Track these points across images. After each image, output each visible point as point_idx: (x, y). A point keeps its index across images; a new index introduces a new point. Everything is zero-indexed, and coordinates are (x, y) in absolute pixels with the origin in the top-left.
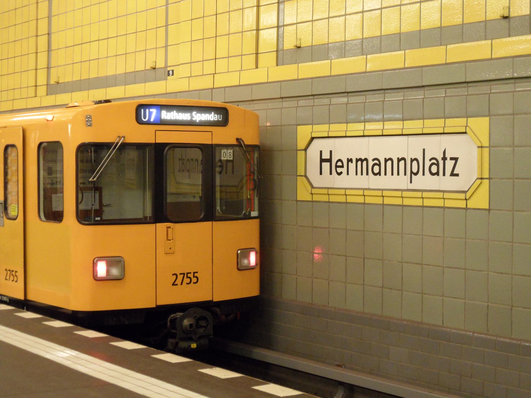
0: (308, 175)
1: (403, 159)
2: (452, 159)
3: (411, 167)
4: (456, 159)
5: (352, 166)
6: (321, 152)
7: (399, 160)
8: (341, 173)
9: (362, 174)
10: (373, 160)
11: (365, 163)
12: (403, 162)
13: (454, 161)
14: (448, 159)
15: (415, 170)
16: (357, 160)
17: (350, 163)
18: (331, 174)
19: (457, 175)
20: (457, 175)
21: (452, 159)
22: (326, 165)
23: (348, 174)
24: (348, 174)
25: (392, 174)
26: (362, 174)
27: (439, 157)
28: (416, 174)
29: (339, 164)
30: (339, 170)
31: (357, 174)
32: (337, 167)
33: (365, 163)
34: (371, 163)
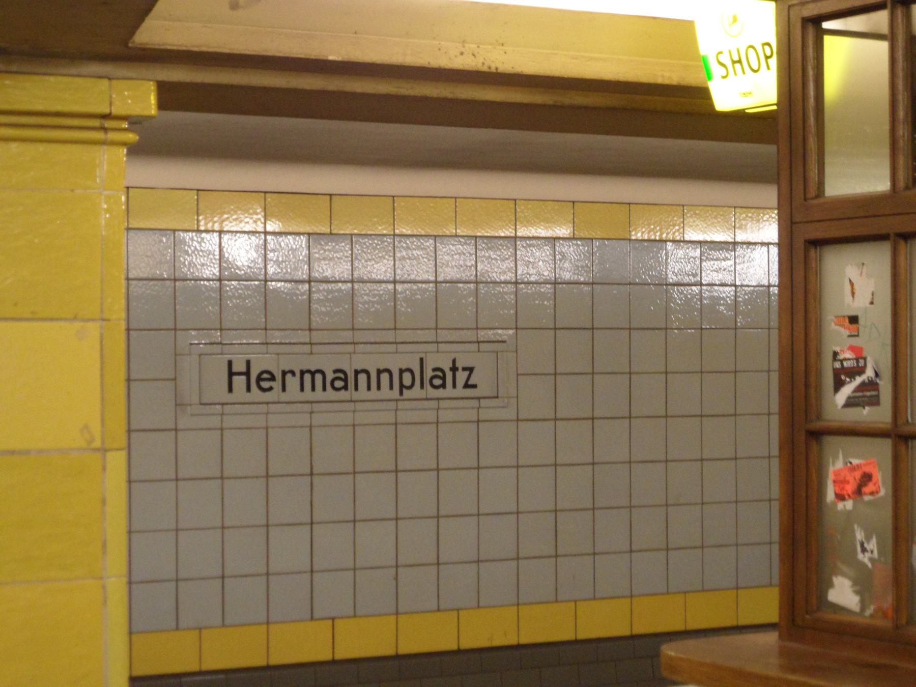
2: (464, 369)
4: (471, 370)
7: (379, 372)
11: (318, 377)
13: (467, 373)
14: (460, 369)
16: (302, 373)
21: (464, 369)
23: (284, 389)
24: (284, 389)
29: (265, 376)
30: (265, 385)
31: (302, 389)
33: (318, 377)
34: (330, 376)
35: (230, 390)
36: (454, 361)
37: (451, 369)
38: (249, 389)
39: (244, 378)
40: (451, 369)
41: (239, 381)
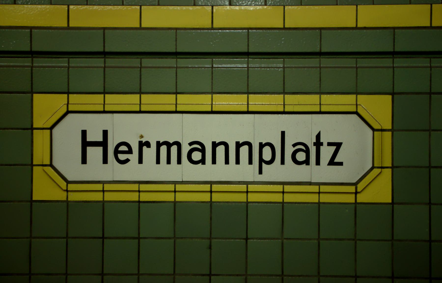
0: (54, 164)
2: (330, 144)
3: (263, 154)
4: (338, 145)
7: (238, 145)
11: (174, 149)
12: (246, 148)
13: (334, 148)
14: (325, 144)
16: (159, 145)
17: (145, 148)
20: (341, 164)
21: (330, 144)
24: (140, 161)
25: (227, 162)
26: (169, 162)
27: (310, 142)
29: (123, 148)
30: (122, 157)
31: (158, 162)
32: (117, 152)
33: (174, 149)
34: (186, 149)
35: (84, 161)
36: (318, 136)
37: (315, 144)
38: (105, 161)
39: (100, 149)
40: (315, 144)
41: (95, 153)
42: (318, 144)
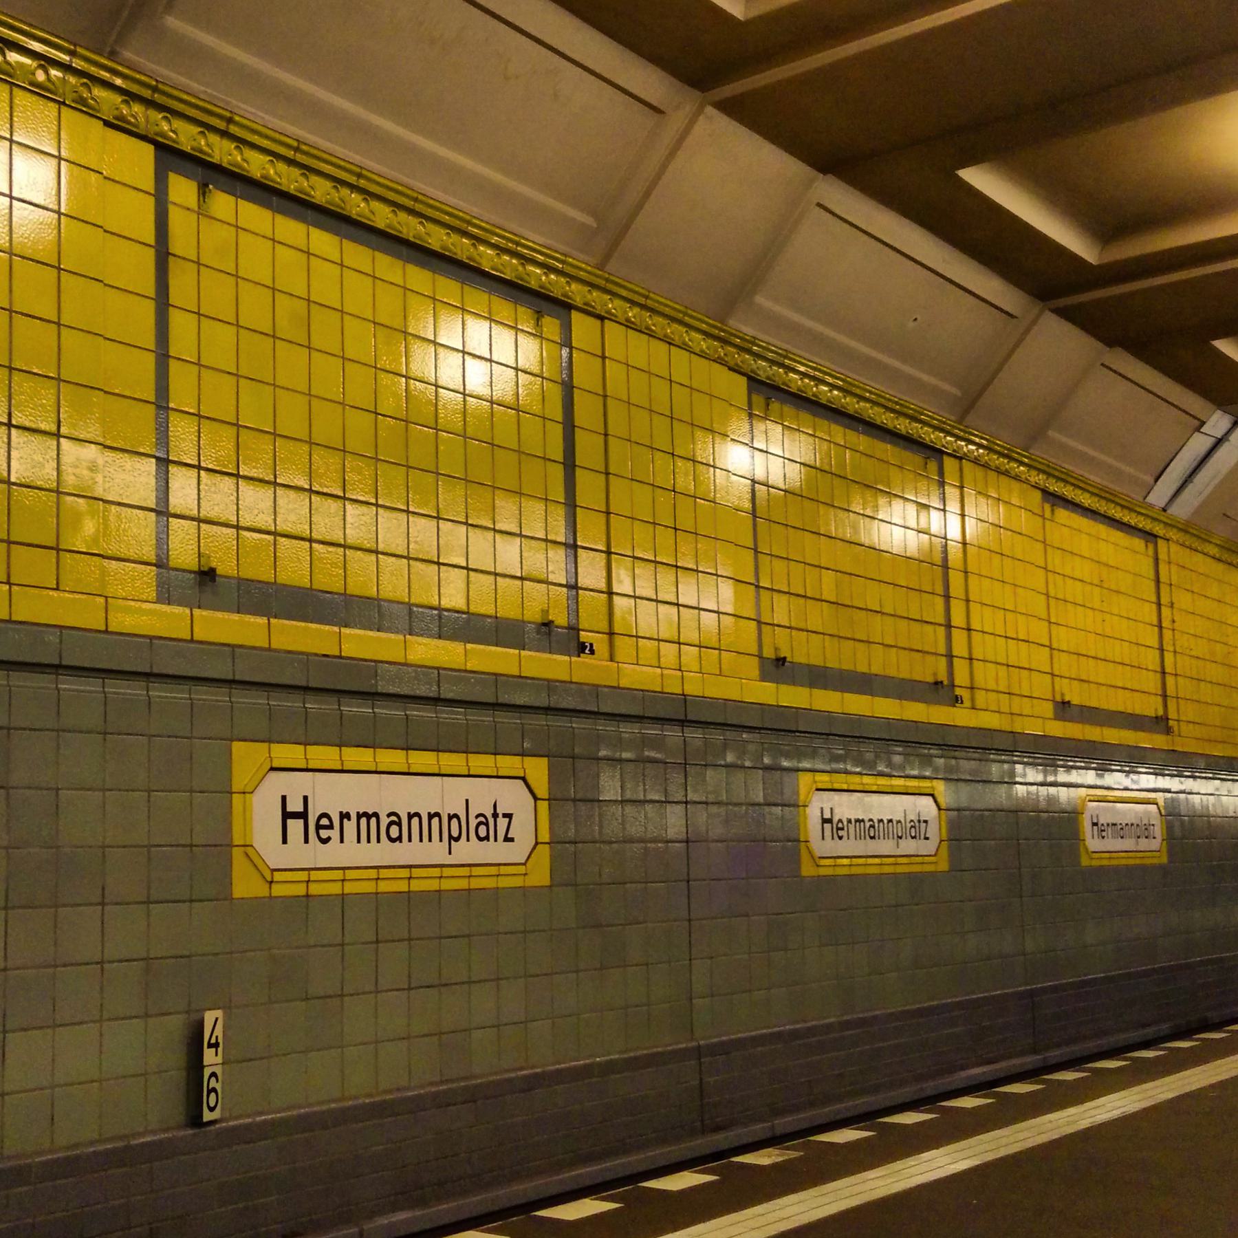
1: (437, 815)
2: (505, 815)
5: (350, 826)
6: (284, 798)
7: (431, 816)
8: (329, 839)
9: (369, 841)
10: (389, 815)
11: (373, 820)
15: (455, 834)
16: (359, 816)
18: (306, 841)
19: (512, 840)
20: (512, 840)
21: (505, 815)
22: (295, 826)
25: (421, 840)
26: (369, 841)
27: (489, 814)
28: (457, 839)
29: (324, 822)
30: (324, 834)
32: (319, 827)
33: (373, 820)
34: (385, 821)
42: (495, 815)
